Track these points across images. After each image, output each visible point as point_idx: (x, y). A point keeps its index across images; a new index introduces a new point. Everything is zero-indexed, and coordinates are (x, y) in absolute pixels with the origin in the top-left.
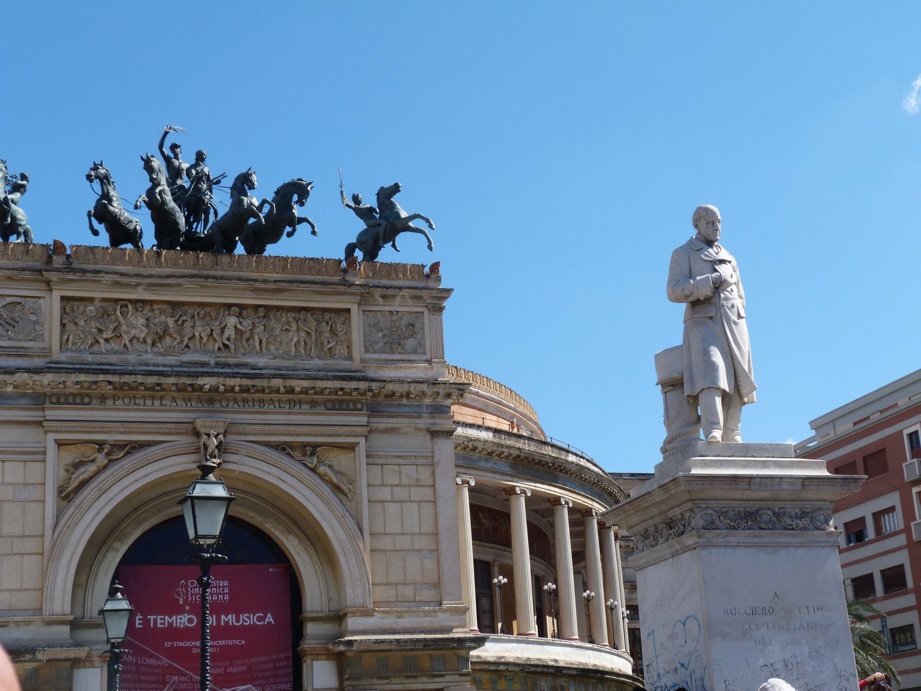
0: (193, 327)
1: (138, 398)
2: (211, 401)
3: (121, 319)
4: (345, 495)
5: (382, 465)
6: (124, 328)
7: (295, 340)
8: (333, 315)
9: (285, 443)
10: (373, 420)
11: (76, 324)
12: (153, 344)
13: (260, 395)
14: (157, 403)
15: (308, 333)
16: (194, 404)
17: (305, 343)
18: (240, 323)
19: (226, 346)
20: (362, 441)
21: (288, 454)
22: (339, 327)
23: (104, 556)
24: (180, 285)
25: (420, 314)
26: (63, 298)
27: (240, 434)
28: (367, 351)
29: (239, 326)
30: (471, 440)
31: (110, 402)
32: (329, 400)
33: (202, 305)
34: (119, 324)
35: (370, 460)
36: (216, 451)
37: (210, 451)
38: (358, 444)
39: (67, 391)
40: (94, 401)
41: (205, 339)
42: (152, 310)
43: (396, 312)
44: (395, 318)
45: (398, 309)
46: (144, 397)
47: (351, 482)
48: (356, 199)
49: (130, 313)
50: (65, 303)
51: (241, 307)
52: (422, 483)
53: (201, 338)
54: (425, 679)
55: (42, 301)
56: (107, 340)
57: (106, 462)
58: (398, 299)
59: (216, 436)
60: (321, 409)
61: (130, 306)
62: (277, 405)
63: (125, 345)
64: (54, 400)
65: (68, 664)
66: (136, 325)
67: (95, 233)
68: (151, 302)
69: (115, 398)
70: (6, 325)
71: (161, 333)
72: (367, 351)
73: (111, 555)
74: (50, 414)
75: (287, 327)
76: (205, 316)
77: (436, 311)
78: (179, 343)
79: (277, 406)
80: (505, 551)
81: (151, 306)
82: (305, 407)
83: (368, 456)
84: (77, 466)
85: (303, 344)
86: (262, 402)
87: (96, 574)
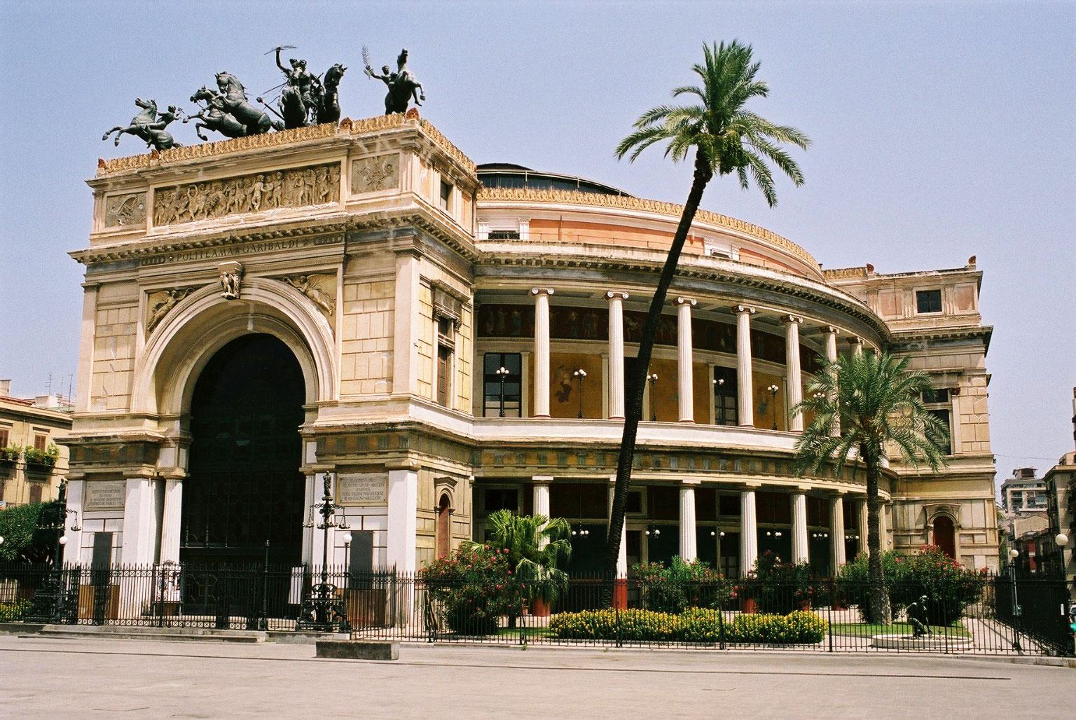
0: (235, 195)
1: (193, 254)
2: (237, 250)
3: (190, 197)
4: (328, 311)
5: (357, 284)
6: (190, 205)
7: (301, 193)
8: (331, 169)
9: (287, 275)
10: (349, 249)
11: (164, 207)
12: (209, 214)
13: (268, 240)
14: (204, 256)
15: (311, 187)
16: (227, 254)
17: (309, 194)
18: (264, 187)
19: (253, 206)
20: (340, 267)
21: (289, 283)
22: (335, 178)
23: (180, 371)
26: (157, 190)
27: (256, 272)
28: (354, 191)
29: (263, 190)
30: (493, 254)
31: (175, 260)
32: (317, 237)
33: (243, 177)
34: (189, 203)
35: (347, 282)
36: (229, 286)
37: (225, 287)
38: (337, 269)
39: (150, 255)
40: (166, 261)
41: (241, 205)
42: (211, 188)
43: (378, 157)
46: (196, 253)
47: (334, 301)
48: (385, 70)
49: (197, 193)
50: (159, 194)
51: (265, 174)
52: (387, 296)
53: (239, 202)
54: (372, 456)
55: (147, 194)
56: (181, 215)
57: (173, 302)
59: (227, 276)
60: (311, 245)
61: (196, 188)
62: (281, 246)
63: (191, 218)
64: (144, 263)
65: (142, 445)
66: (199, 201)
67: (205, 138)
68: (210, 182)
69: (179, 256)
70: (126, 215)
71: (213, 203)
72: (354, 191)
73: (185, 368)
74: (143, 273)
75: (297, 184)
76: (243, 185)
77: (408, 150)
78: (226, 209)
79: (281, 247)
80: (660, 347)
81: (211, 185)
82: (301, 246)
83: (344, 279)
84: (159, 306)
85: (306, 195)
86: (271, 245)
87: (176, 383)
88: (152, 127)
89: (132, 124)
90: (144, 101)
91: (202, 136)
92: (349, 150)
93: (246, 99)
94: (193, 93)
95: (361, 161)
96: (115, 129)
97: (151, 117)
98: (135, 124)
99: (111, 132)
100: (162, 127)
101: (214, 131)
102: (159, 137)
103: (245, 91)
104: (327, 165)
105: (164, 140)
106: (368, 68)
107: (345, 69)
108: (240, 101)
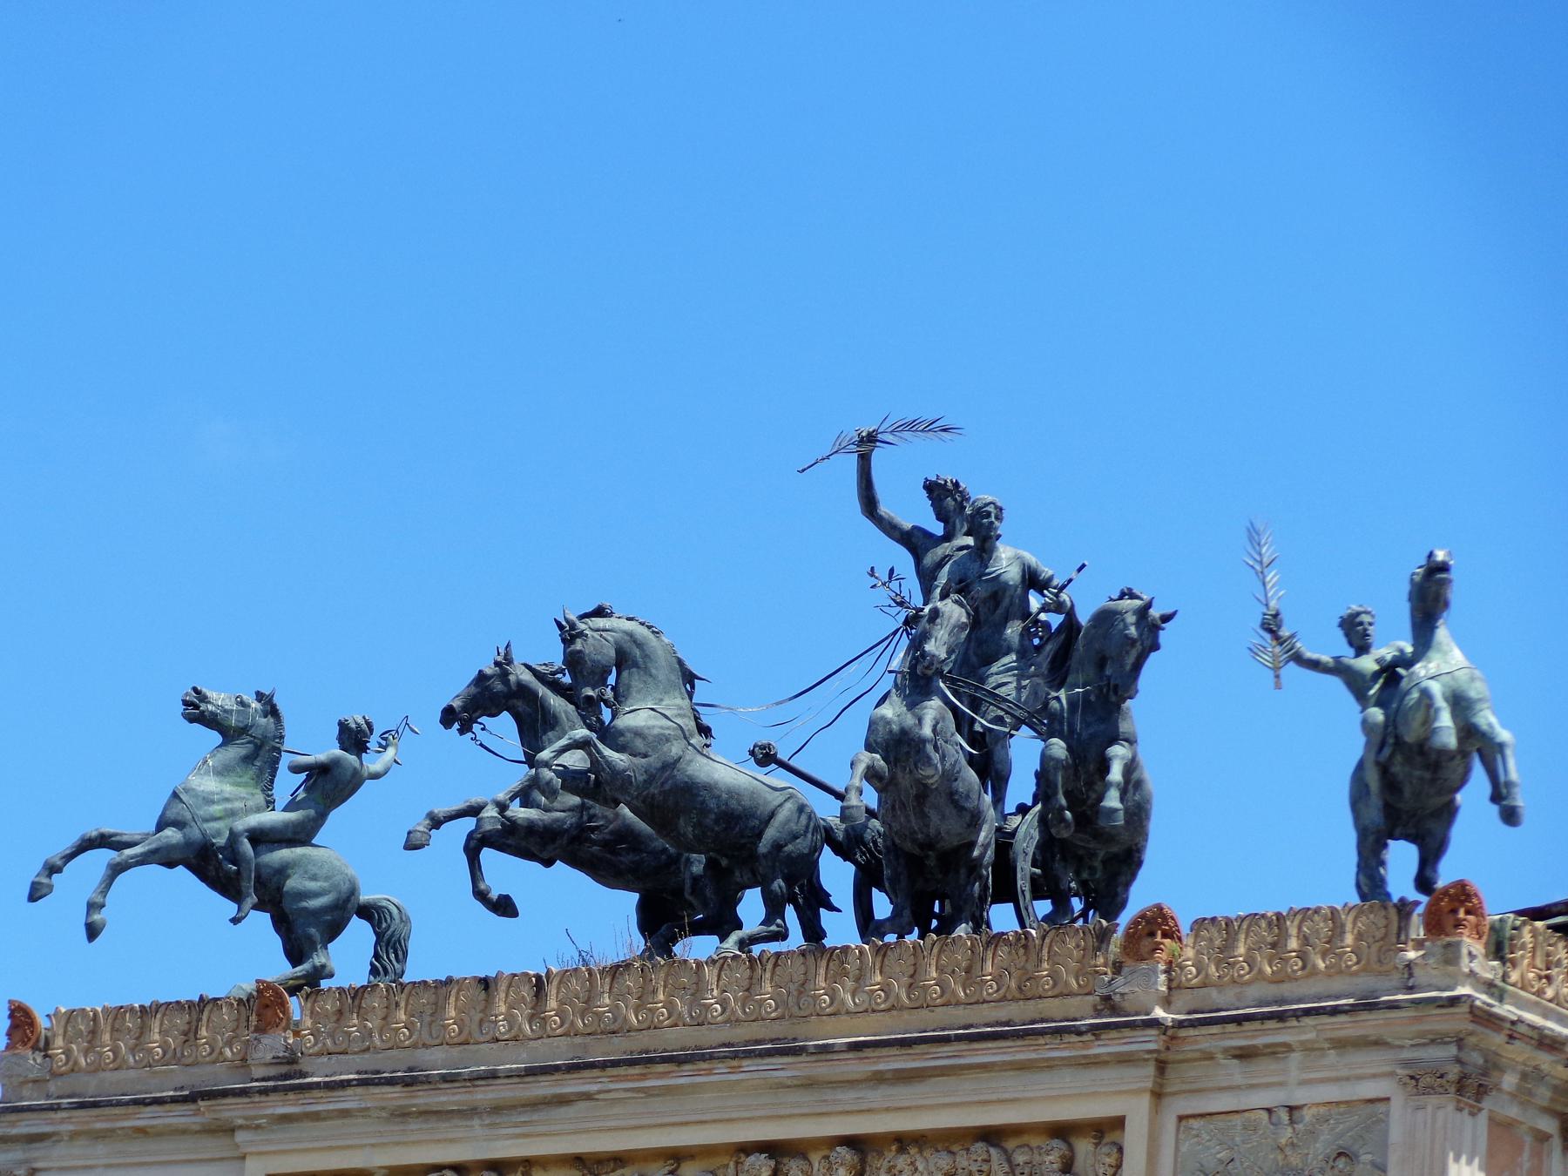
8: (1083, 1147)
24: (588, 1097)
25: (1381, 1107)
44: (1287, 1134)
45: (1299, 1096)
48: (1356, 632)
58: (1296, 1057)
67: (504, 907)
77: (1429, 1090)
88: (260, 838)
89: (161, 826)
90: (220, 699)
91: (494, 895)
92: (1162, 1066)
93: (705, 731)
94: (454, 688)
95: (1219, 1122)
96: (88, 844)
97: (258, 778)
98: (179, 824)
99: (69, 857)
100: (300, 835)
101: (548, 863)
102: (292, 883)
103: (702, 692)
104: (1062, 1131)
105: (316, 895)
106: (1271, 626)
107: (1166, 618)
108: (675, 749)
